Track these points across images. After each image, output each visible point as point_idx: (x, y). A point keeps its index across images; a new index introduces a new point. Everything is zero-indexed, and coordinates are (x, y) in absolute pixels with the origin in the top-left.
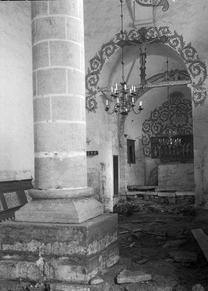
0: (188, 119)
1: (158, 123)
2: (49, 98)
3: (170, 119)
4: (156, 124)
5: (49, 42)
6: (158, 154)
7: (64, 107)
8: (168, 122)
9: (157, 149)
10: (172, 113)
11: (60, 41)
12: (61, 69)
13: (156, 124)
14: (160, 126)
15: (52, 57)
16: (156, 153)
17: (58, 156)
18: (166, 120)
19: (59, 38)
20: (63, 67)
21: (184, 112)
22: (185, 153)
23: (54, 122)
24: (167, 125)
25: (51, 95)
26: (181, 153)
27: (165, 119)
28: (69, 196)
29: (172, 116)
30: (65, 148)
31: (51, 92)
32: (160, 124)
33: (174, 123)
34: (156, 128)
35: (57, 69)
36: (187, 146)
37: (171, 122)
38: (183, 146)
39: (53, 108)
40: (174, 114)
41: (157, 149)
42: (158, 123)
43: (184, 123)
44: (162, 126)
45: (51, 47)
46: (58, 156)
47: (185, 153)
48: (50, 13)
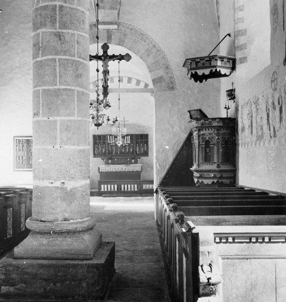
2: (55, 122)
5: (57, 60)
7: (73, 132)
11: (70, 60)
12: (70, 90)
15: (60, 76)
17: (66, 185)
19: (69, 55)
20: (73, 88)
23: (62, 148)
25: (58, 118)
28: (78, 230)
30: (72, 176)
31: (58, 115)
35: (66, 89)
39: (61, 132)
45: (60, 65)
46: (66, 185)
48: (59, 28)
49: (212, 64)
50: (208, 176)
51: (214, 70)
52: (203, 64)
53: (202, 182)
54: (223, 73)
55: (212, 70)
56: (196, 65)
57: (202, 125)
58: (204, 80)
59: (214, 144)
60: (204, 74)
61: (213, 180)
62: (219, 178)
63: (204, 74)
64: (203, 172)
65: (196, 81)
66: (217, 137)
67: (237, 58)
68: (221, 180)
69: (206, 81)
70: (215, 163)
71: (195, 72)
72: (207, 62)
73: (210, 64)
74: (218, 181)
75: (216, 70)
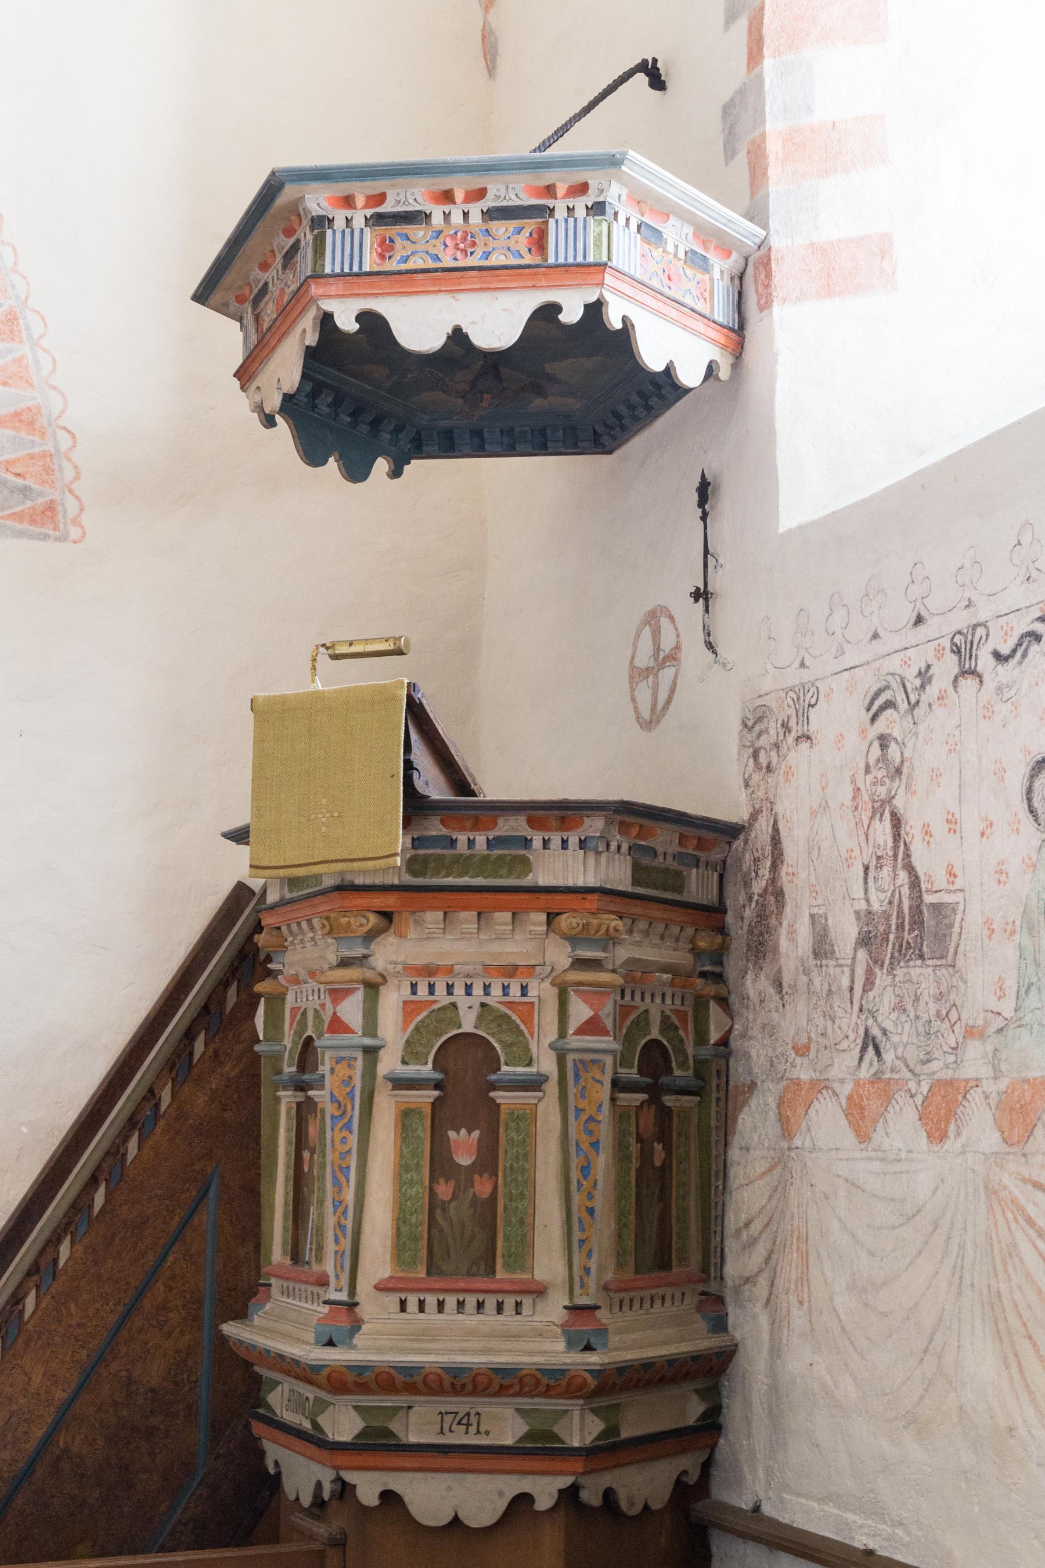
49: (557, 251)
50: (458, 1437)
51: (572, 314)
52: (468, 241)
53: (389, 1497)
54: (653, 360)
55: (550, 311)
56: (386, 248)
57: (414, 865)
58: (381, 465)
59: (535, 1084)
60: (458, 336)
61: (513, 1485)
62: (587, 1453)
63: (458, 336)
64: (411, 1388)
65: (313, 457)
66: (580, 1011)
67: (777, 243)
68: (606, 1480)
69: (396, 473)
70: (539, 1291)
71: (364, 317)
72: (501, 228)
73: (540, 242)
74: (569, 1496)
75: (595, 310)
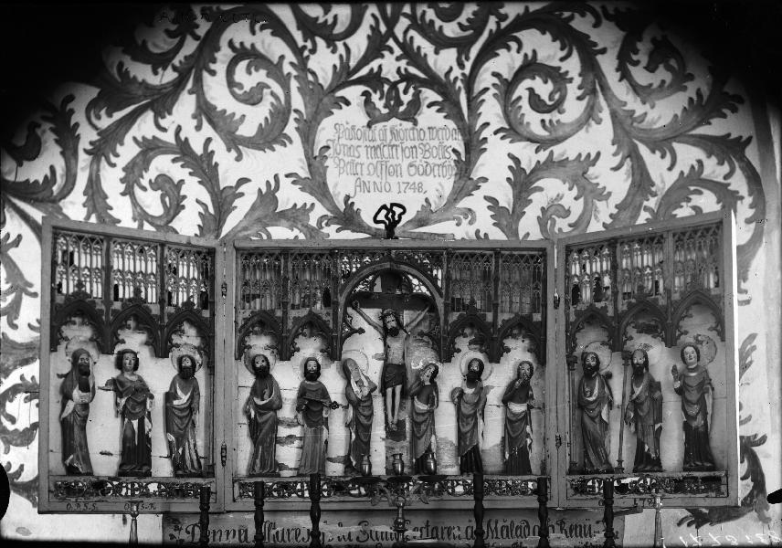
0: (474, 144)
1: (182, 150)
3: (308, 134)
4: (150, 148)
6: (135, 453)
8: (290, 157)
9: (132, 397)
10: (324, 62)
13: (150, 148)
14: (194, 191)
16: (105, 434)
18: (269, 137)
21: (444, 61)
22: (470, 458)
24: (268, 197)
26: (423, 466)
27: (253, 119)
29: (324, 100)
32: (204, 168)
33: (340, 183)
34: (152, 202)
36: (498, 378)
37: (316, 162)
38: (452, 377)
40: (344, 76)
41: (132, 397)
42: (182, 150)
43: (440, 185)
44: (223, 201)
47: (470, 458)
